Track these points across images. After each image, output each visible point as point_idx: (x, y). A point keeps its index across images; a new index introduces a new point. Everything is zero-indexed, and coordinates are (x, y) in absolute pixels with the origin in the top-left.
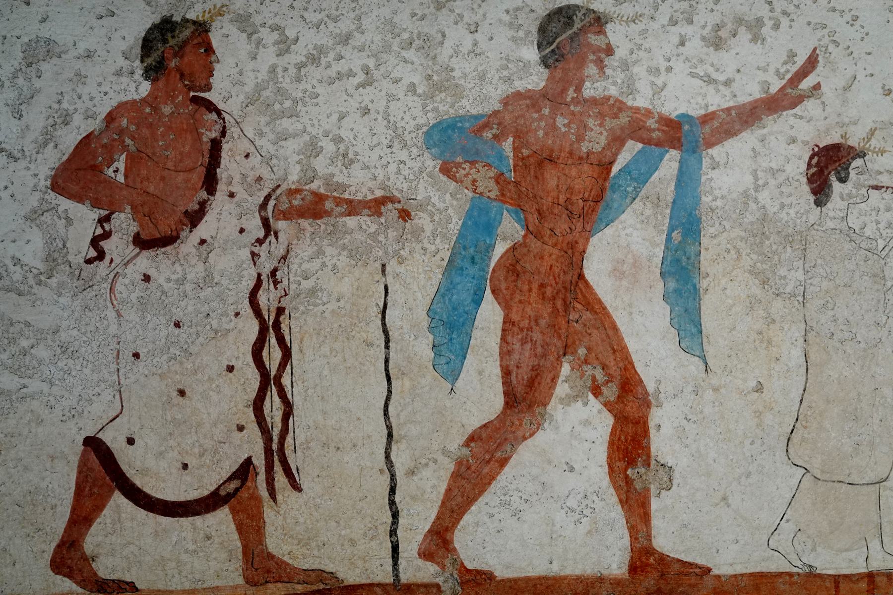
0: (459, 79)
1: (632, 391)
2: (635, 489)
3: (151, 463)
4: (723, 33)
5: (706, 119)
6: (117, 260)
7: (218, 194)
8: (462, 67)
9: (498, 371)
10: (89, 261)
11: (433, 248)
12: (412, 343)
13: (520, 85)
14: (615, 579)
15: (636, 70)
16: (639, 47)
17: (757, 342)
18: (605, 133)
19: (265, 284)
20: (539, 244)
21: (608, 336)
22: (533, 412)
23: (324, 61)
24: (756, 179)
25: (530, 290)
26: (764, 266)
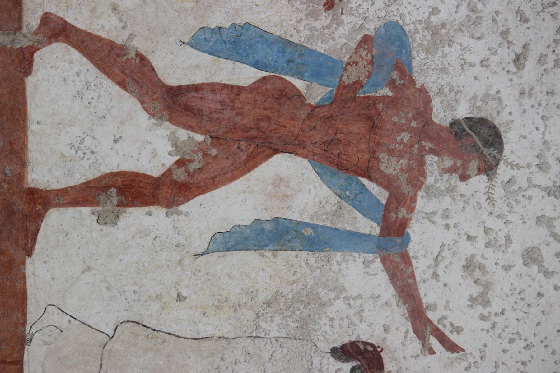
0: (443, 51)
1: (180, 192)
2: (99, 195)
4: (477, 273)
5: (406, 258)
8: (452, 53)
11: (301, 28)
12: (222, 10)
13: (436, 103)
14: (24, 177)
15: (448, 199)
16: (467, 202)
17: (219, 297)
18: (394, 173)
20: (303, 117)
21: (226, 173)
22: (164, 111)
25: (265, 109)
26: (282, 304)
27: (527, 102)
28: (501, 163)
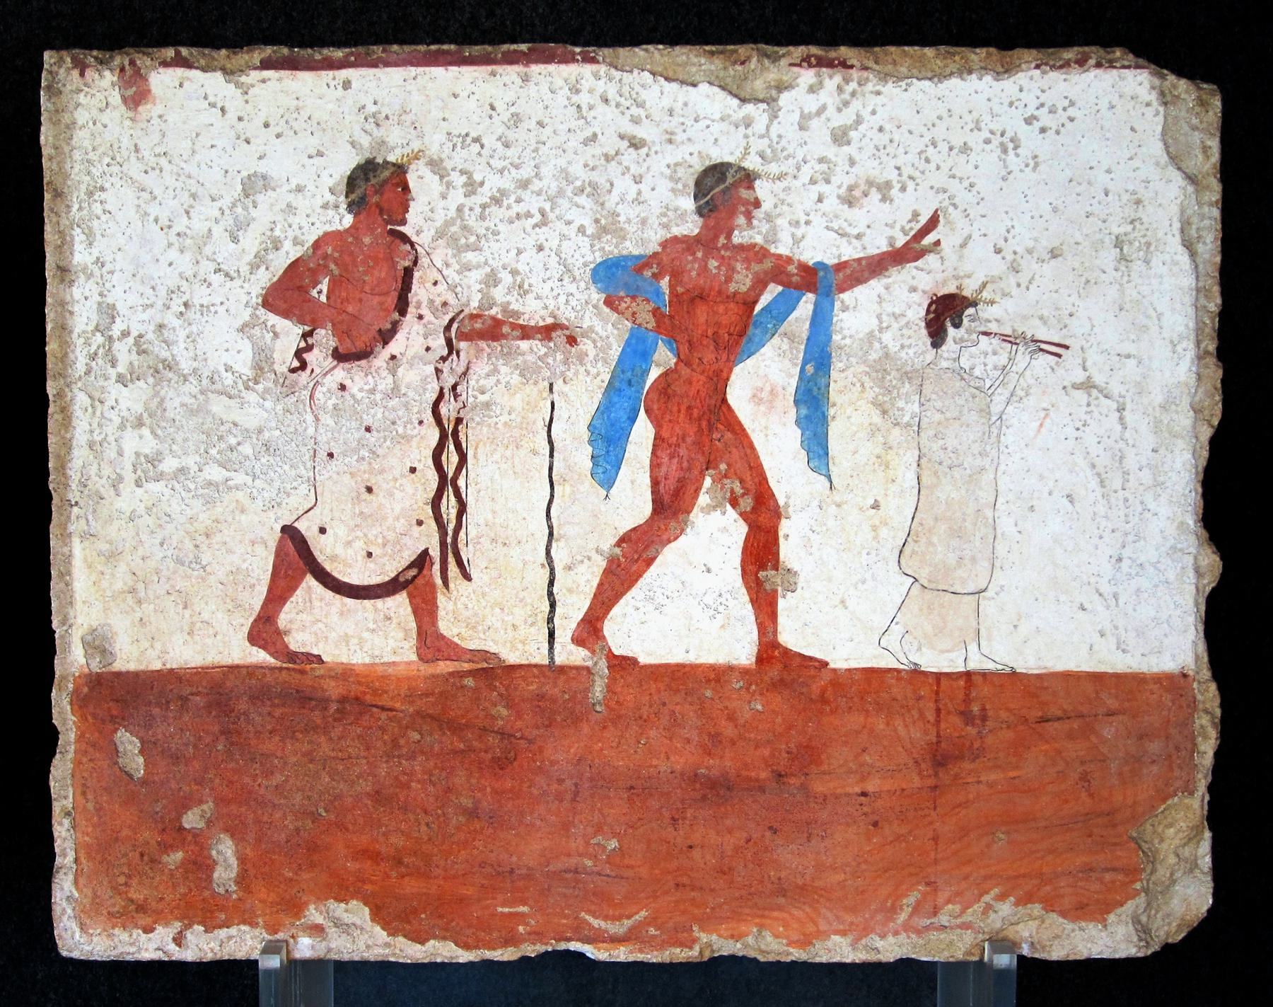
3: (339, 550)
5: (840, 267)
6: (317, 371)
7: (408, 316)
8: (626, 213)
9: (648, 481)
10: (293, 371)
11: (595, 371)
13: (677, 231)
15: (779, 221)
16: (783, 202)
19: (447, 396)
20: (688, 371)
23: (505, 203)
24: (881, 323)
25: (679, 411)
27: (680, 137)
28: (743, 165)
